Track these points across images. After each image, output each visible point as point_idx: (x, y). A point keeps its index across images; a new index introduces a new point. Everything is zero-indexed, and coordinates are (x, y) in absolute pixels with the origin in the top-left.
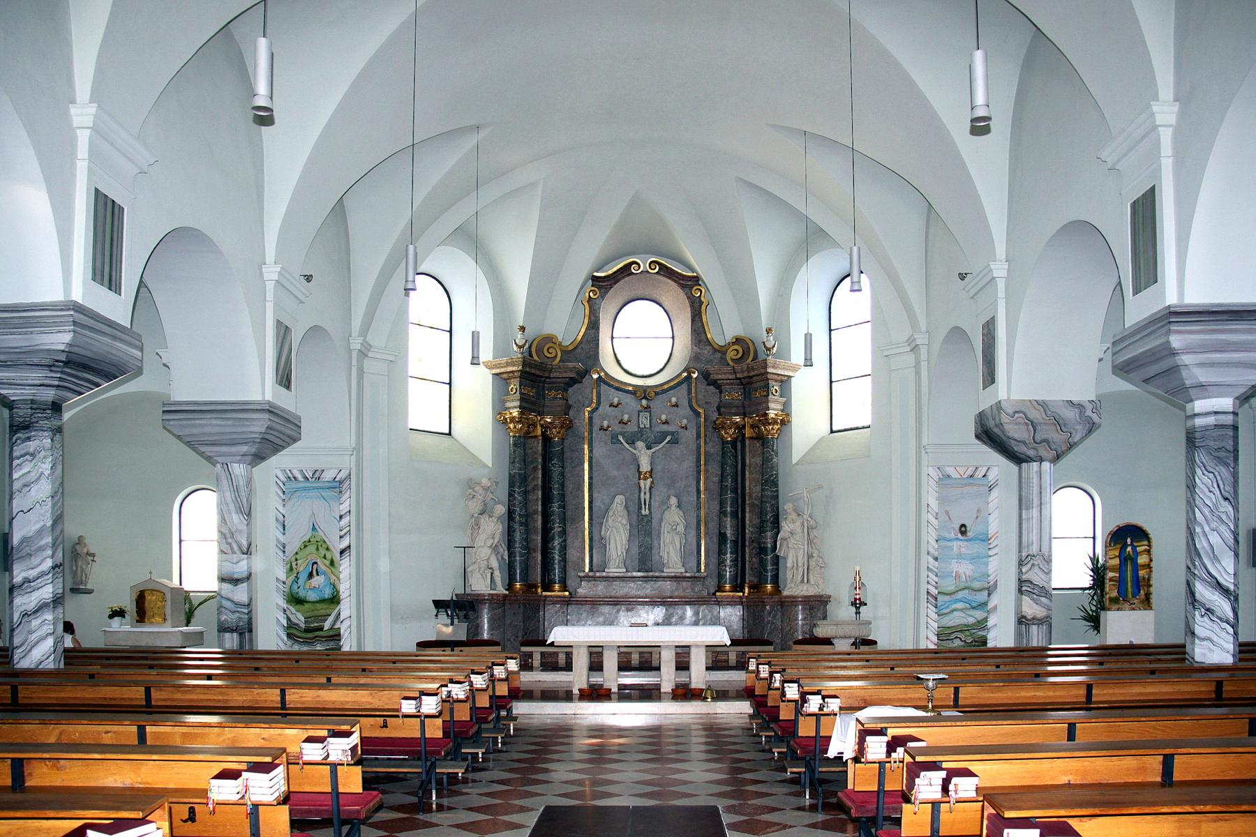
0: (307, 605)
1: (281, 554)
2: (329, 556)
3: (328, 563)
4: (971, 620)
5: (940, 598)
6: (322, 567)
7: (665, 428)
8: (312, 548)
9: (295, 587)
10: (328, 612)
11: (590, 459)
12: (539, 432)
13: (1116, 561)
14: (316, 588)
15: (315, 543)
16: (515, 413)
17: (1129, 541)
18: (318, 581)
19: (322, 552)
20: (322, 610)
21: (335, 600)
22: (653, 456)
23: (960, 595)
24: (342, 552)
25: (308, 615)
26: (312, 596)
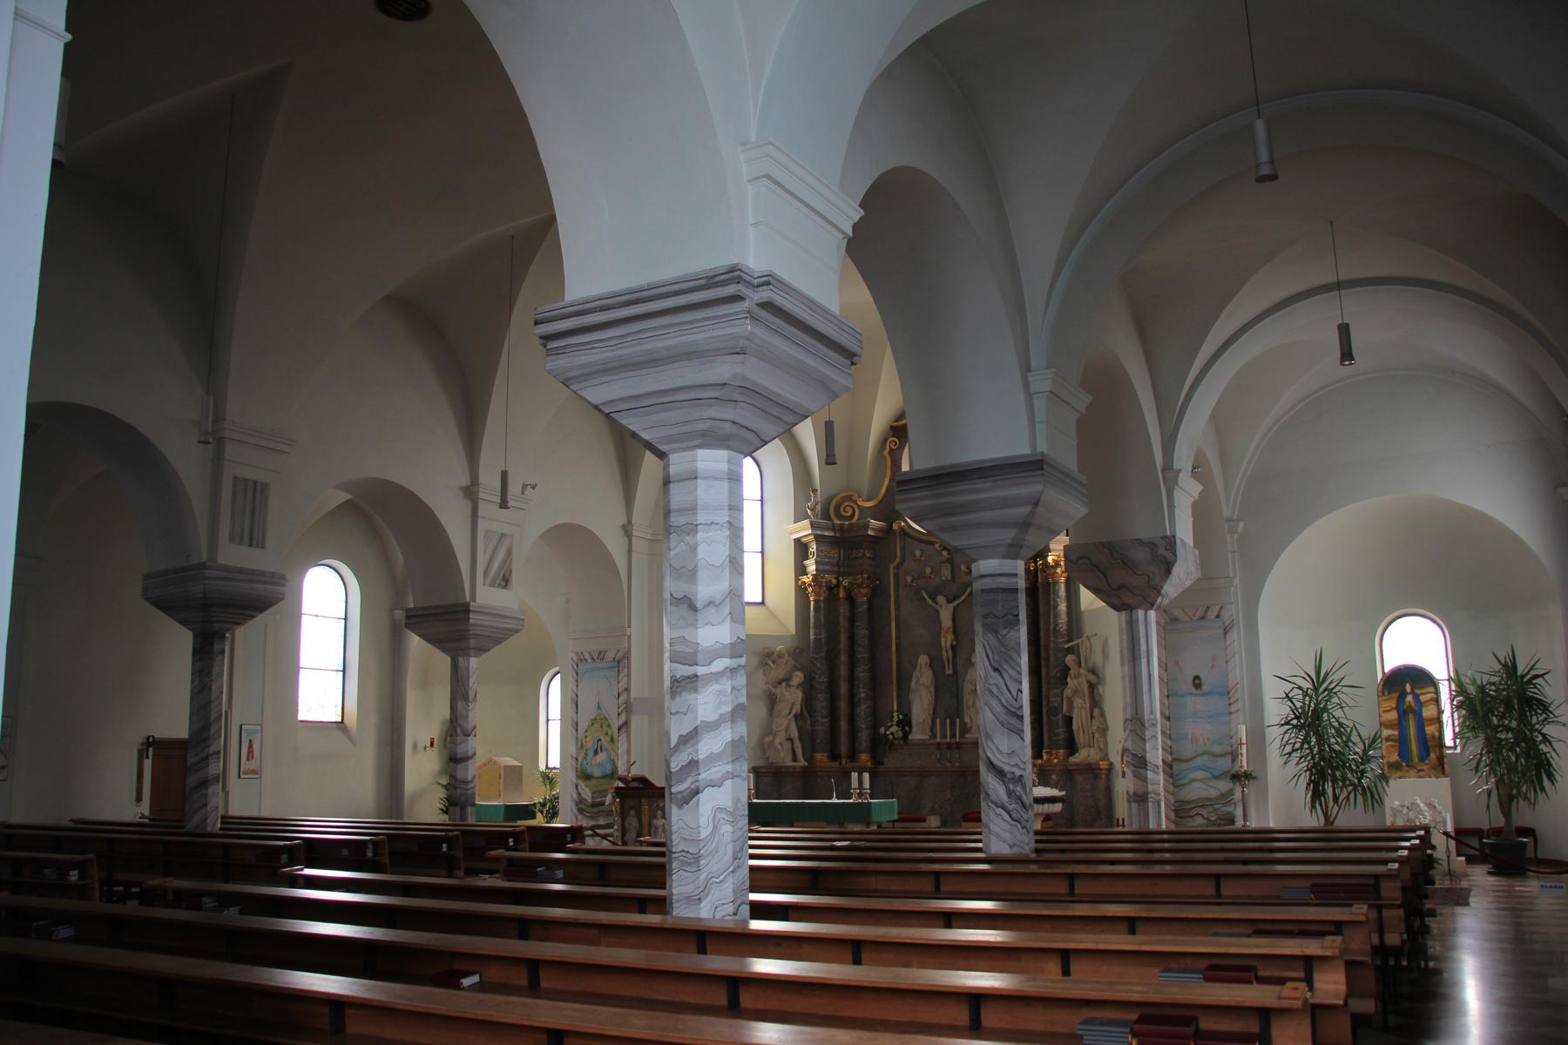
0: (594, 782)
4: (1213, 793)
5: (1175, 765)
6: (605, 744)
8: (597, 725)
11: (897, 617)
13: (1394, 715)
15: (600, 721)
17: (1408, 688)
18: (602, 757)
23: (1200, 761)
26: (597, 772)
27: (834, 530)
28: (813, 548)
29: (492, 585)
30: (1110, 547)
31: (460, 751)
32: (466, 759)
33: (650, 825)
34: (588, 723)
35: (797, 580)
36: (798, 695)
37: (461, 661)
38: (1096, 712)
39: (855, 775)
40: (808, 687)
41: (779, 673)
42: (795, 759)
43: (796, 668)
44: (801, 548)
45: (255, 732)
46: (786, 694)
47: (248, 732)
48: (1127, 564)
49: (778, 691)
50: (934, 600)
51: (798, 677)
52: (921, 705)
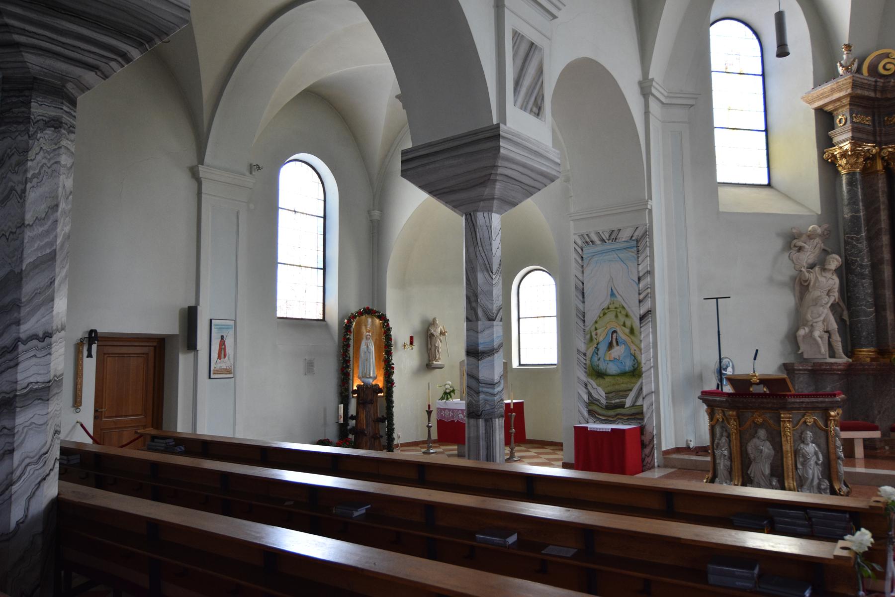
0: (608, 379)
1: (581, 324)
2: (628, 323)
3: (627, 331)
8: (611, 316)
9: (596, 359)
10: (629, 386)
12: (879, 166)
14: (615, 359)
15: (614, 309)
16: (847, 146)
18: (617, 351)
19: (622, 319)
20: (623, 383)
21: (635, 372)
24: (642, 318)
25: (610, 389)
26: (613, 369)
27: (875, 91)
28: (842, 117)
29: (524, 108)
31: (483, 341)
32: (491, 352)
33: (796, 453)
35: (821, 153)
36: (835, 282)
37: (480, 217)
40: (846, 272)
41: (809, 255)
42: (833, 354)
43: (825, 252)
44: (825, 119)
45: (228, 328)
46: (821, 279)
47: (220, 328)
49: (811, 277)
51: (834, 262)
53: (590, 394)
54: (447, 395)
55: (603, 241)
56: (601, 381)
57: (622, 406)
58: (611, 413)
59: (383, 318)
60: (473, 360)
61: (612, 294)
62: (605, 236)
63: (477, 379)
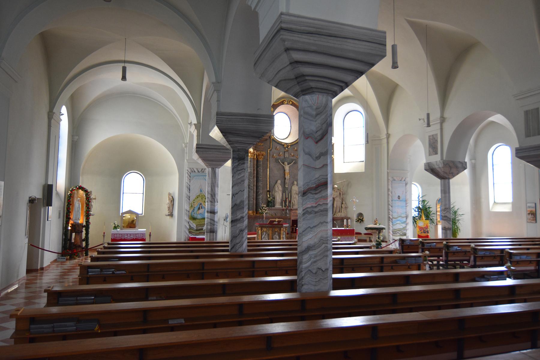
0: (197, 220)
4: (401, 227)
7: (292, 158)
8: (200, 198)
15: (201, 196)
22: (289, 167)
23: (399, 218)
30: (453, 162)
34: (195, 197)
38: (344, 202)
39: (345, 220)
48: (457, 167)
50: (283, 163)
52: (278, 196)
53: (190, 226)
54: (115, 228)
55: (199, 172)
56: (194, 221)
57: (202, 229)
58: (198, 232)
59: (86, 191)
60: (212, 215)
61: (201, 191)
62: (200, 170)
63: (214, 221)
